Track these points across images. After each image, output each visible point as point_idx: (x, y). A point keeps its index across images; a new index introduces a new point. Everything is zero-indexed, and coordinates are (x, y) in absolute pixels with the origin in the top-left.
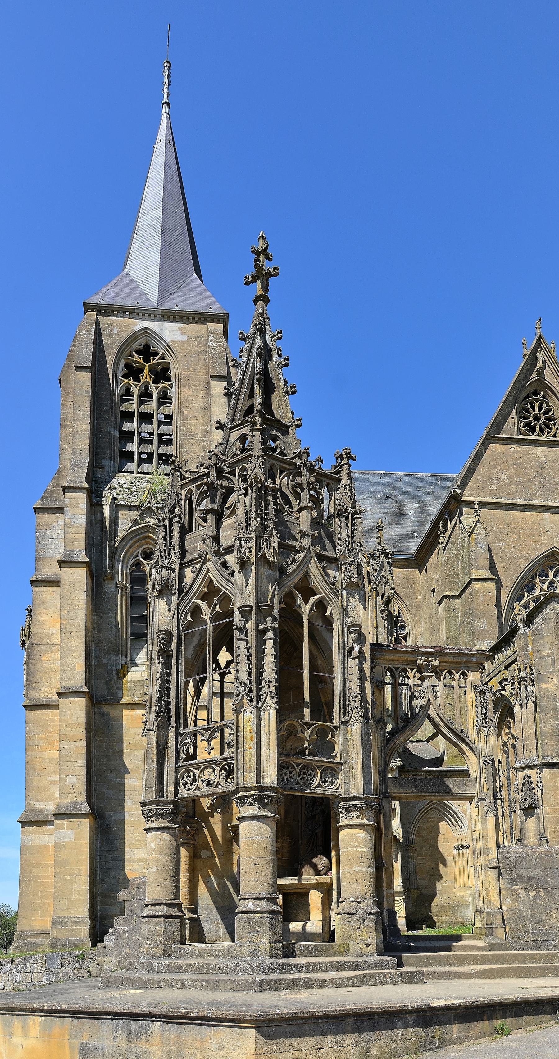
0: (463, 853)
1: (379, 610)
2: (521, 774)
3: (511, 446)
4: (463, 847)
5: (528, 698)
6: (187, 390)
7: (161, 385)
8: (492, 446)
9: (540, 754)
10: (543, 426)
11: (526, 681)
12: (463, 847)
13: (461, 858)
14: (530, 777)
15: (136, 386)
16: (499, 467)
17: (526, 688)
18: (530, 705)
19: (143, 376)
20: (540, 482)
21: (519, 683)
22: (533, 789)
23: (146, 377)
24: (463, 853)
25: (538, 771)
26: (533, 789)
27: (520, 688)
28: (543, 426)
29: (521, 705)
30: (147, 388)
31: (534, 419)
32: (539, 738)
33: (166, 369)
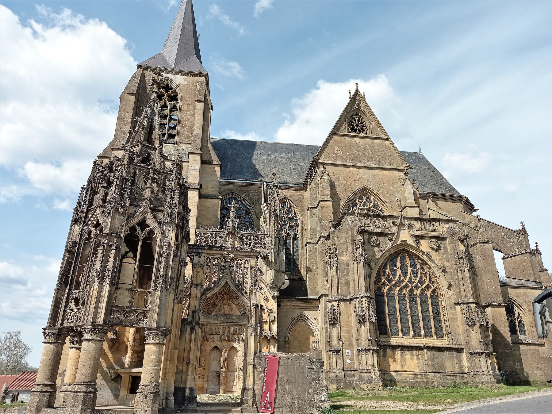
1: (271, 214)
3: (344, 138)
6: (185, 106)
7: (172, 103)
8: (334, 137)
15: (160, 103)
19: (164, 98)
20: (358, 155)
23: (165, 98)
29: (331, 268)
30: (165, 103)
31: (359, 125)
33: (176, 95)
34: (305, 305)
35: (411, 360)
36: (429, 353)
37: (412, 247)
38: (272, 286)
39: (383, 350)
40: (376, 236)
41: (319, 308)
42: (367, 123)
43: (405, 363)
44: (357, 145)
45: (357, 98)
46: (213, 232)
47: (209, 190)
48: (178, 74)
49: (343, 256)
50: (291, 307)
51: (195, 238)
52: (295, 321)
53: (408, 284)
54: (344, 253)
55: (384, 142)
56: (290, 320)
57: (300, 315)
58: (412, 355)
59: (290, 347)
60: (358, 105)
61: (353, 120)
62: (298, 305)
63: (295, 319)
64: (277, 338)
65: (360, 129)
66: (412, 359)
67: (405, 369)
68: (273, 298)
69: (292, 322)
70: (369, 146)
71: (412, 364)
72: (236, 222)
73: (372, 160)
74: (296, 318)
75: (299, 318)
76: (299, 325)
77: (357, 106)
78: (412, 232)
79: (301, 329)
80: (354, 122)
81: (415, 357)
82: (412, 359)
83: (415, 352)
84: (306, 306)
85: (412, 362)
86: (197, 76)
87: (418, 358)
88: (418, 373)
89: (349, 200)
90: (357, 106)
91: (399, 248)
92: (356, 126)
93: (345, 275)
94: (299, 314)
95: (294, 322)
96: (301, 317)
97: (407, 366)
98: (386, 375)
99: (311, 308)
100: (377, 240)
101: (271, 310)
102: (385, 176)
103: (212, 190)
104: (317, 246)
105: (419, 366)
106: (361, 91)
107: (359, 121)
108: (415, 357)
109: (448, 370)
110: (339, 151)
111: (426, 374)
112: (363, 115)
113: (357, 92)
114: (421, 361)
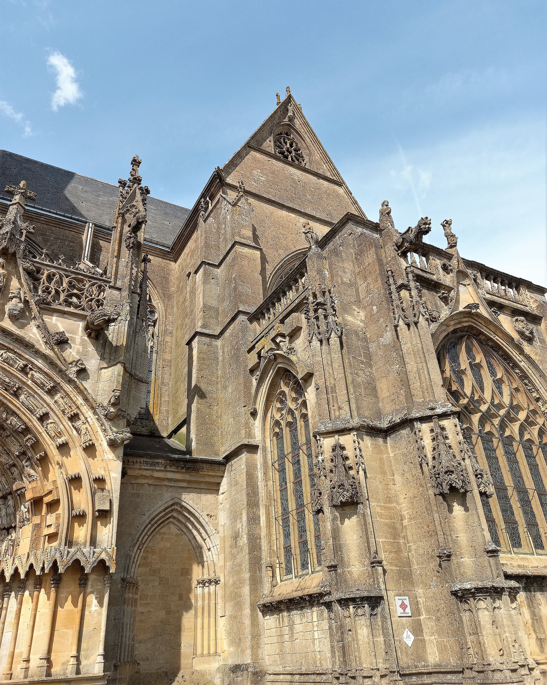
0: (209, 593)
2: (328, 443)
4: (210, 582)
5: (329, 331)
8: (253, 153)
9: (355, 413)
11: (325, 310)
12: (210, 582)
13: (206, 602)
14: (343, 448)
17: (326, 317)
18: (334, 339)
21: (316, 311)
22: (351, 468)
24: (209, 593)
25: (355, 438)
26: (351, 468)
27: (317, 318)
32: (351, 390)
34: (187, 477)
38: (112, 410)
41: (224, 486)
42: (304, 152)
49: (352, 315)
50: (150, 482)
52: (156, 523)
54: (354, 307)
55: (336, 187)
56: (145, 518)
57: (172, 505)
59: (136, 600)
60: (291, 119)
61: (282, 140)
62: (170, 475)
63: (157, 516)
64: (112, 570)
65: (294, 159)
68: (112, 444)
69: (150, 523)
74: (159, 514)
75: (167, 514)
76: (164, 534)
79: (168, 545)
80: (284, 144)
84: (189, 482)
89: (282, 266)
90: (290, 120)
93: (362, 363)
94: (170, 503)
95: (152, 526)
96: (172, 511)
99: (202, 486)
101: (100, 481)
104: (219, 343)
106: (297, 98)
107: (291, 146)
110: (262, 178)
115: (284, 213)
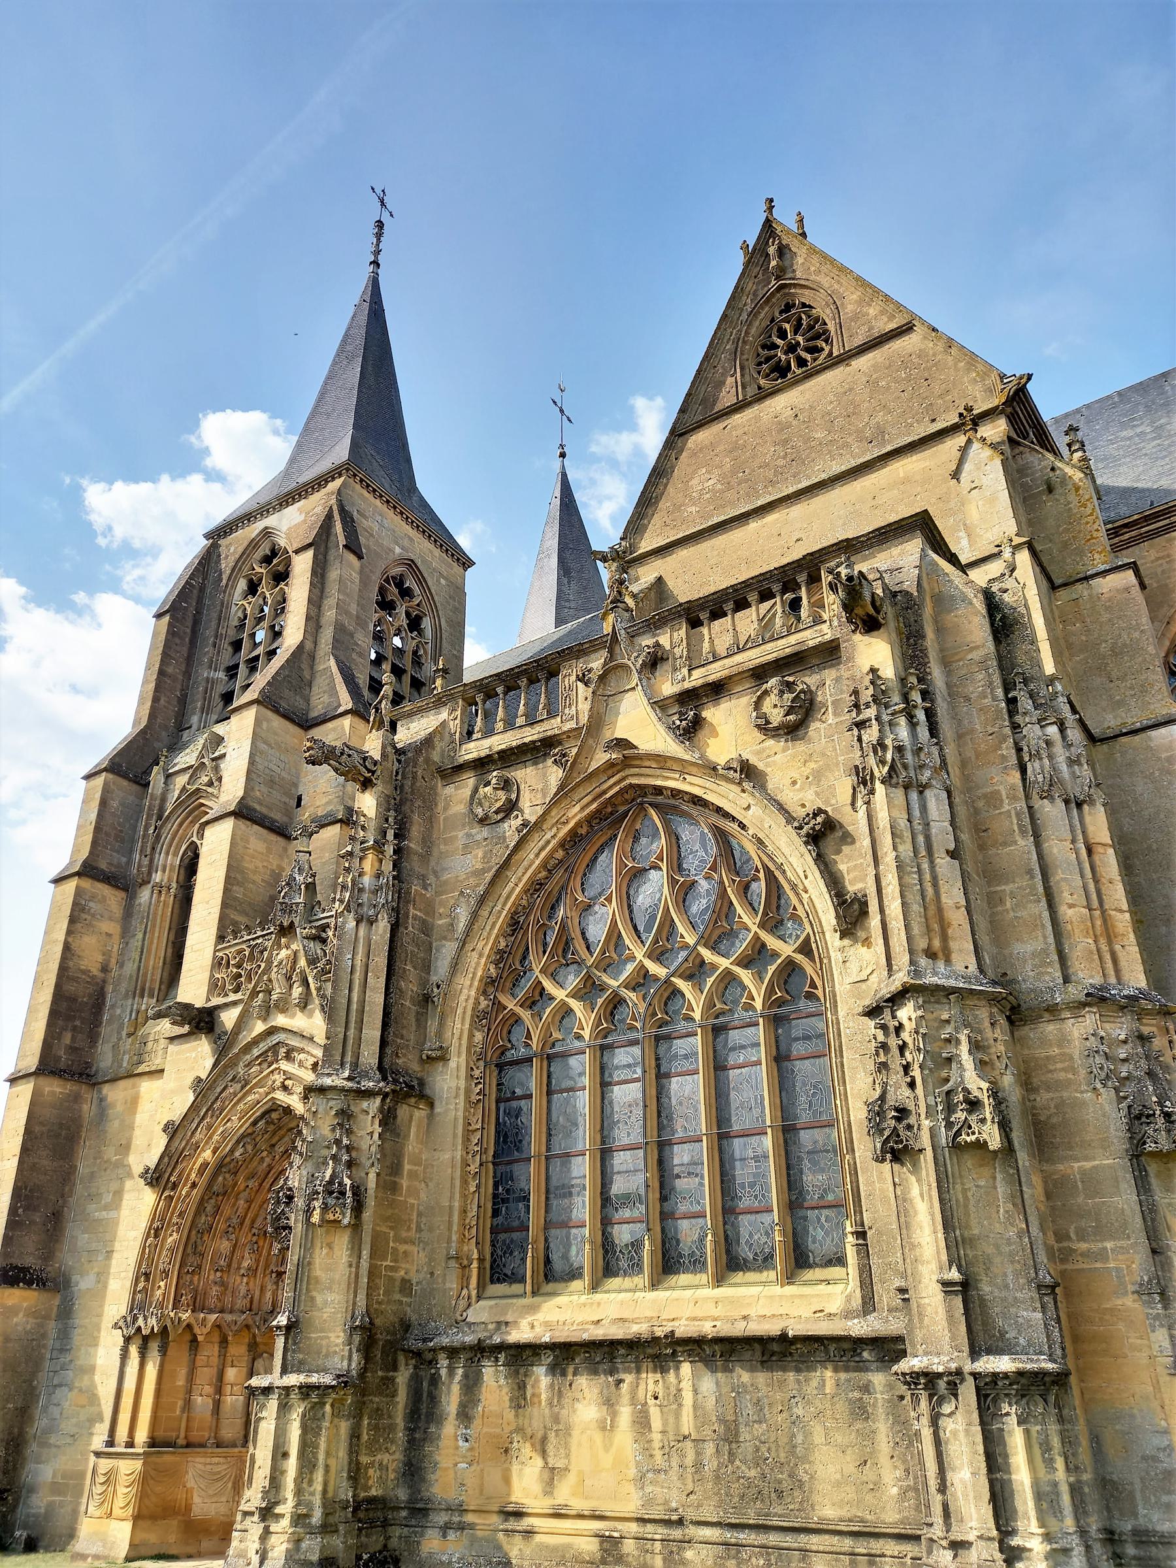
10: (811, 343)
16: (704, 470)
20: (784, 458)
28: (811, 343)
35: (598, 1437)
36: (708, 1383)
37: (662, 761)
39: (466, 1376)
40: (495, 774)
43: (568, 1456)
44: (780, 423)
45: (772, 250)
46: (253, 939)
47: (318, 803)
48: (288, 505)
51: (212, 976)
53: (654, 968)
58: (609, 1403)
66: (607, 1427)
67: (564, 1494)
70: (831, 397)
71: (607, 1460)
72: (303, 887)
73: (846, 445)
77: (778, 278)
78: (668, 688)
81: (625, 1413)
82: (607, 1427)
83: (629, 1378)
85: (607, 1449)
86: (327, 482)
87: (642, 1422)
88: (633, 1527)
91: (605, 792)
92: (786, 353)
97: (572, 1478)
98: (452, 1535)
100: (506, 785)
102: (906, 481)
103: (324, 801)
105: (640, 1480)
106: (785, 218)
108: (625, 1413)
109: (828, 1510)
111: (677, 1533)
112: (805, 296)
113: (769, 229)
114: (656, 1437)
115: (754, 525)
